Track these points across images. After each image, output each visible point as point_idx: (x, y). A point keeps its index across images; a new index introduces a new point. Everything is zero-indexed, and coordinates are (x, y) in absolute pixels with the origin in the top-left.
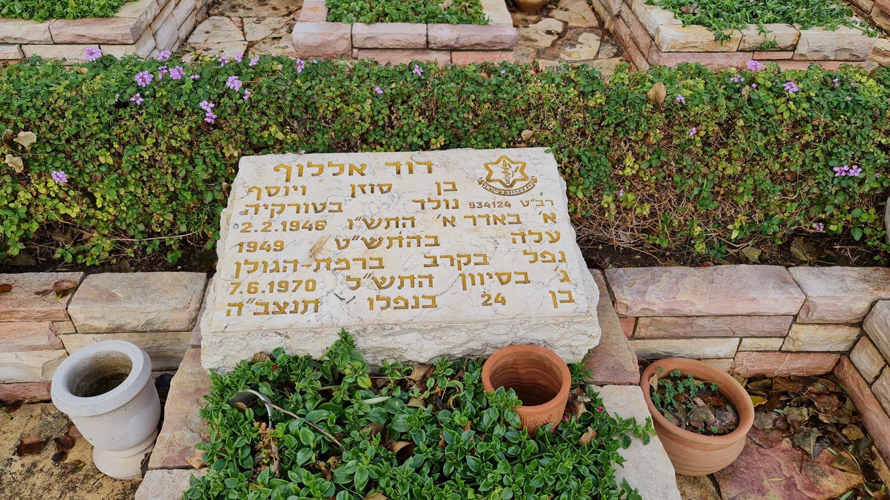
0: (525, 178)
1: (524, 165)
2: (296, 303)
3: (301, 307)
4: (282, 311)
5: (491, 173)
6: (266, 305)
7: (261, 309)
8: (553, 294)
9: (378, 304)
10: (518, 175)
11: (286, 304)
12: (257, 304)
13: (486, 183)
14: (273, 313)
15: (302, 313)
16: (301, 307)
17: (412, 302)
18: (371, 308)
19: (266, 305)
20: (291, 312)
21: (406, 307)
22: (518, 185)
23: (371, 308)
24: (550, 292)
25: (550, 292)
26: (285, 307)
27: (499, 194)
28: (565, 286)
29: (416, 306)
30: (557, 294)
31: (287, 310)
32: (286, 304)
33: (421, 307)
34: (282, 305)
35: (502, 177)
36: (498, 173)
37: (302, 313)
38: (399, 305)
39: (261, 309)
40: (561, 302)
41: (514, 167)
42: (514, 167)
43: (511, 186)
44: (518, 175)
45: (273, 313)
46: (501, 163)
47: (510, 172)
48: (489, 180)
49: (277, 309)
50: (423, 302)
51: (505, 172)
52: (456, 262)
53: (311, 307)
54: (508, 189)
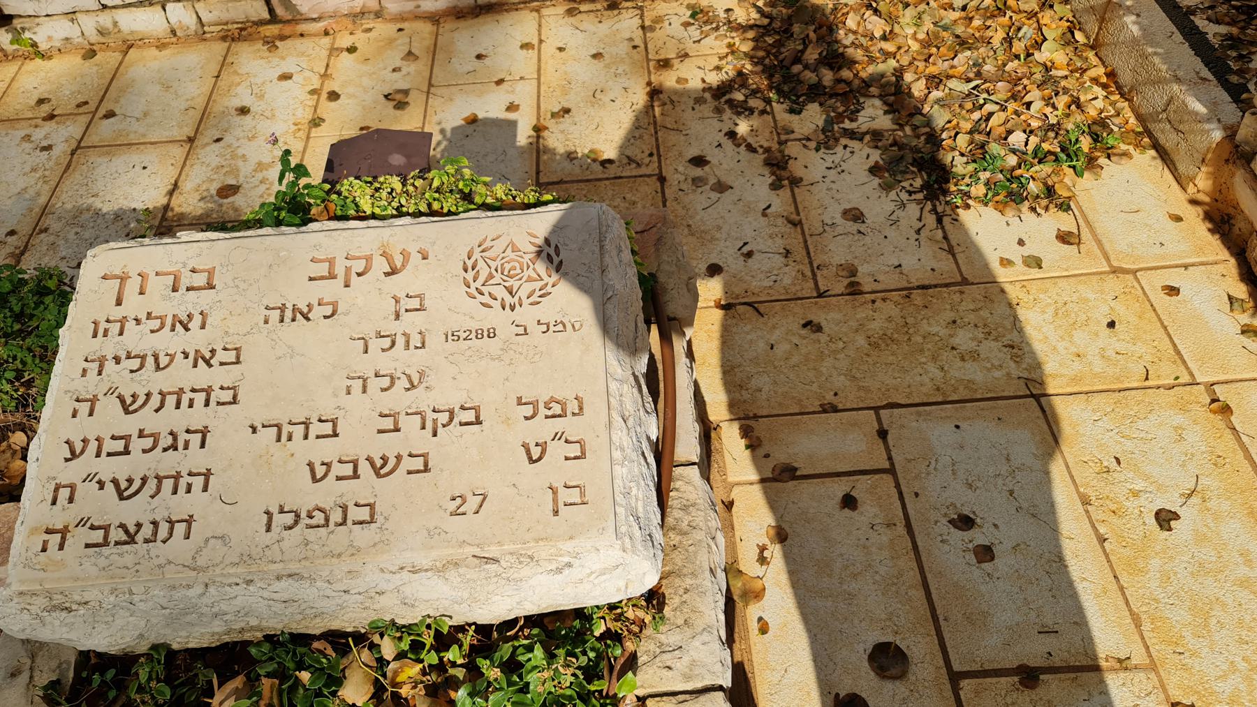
2: (155, 524)
4: (131, 540)
6: (106, 528)
7: (98, 536)
12: (93, 528)
17: (336, 516)
19: (106, 528)
20: (147, 541)
28: (574, 472)
30: (561, 491)
34: (132, 529)
38: (313, 522)
39: (98, 536)
49: (125, 538)
52: (429, 425)
53: (180, 529)
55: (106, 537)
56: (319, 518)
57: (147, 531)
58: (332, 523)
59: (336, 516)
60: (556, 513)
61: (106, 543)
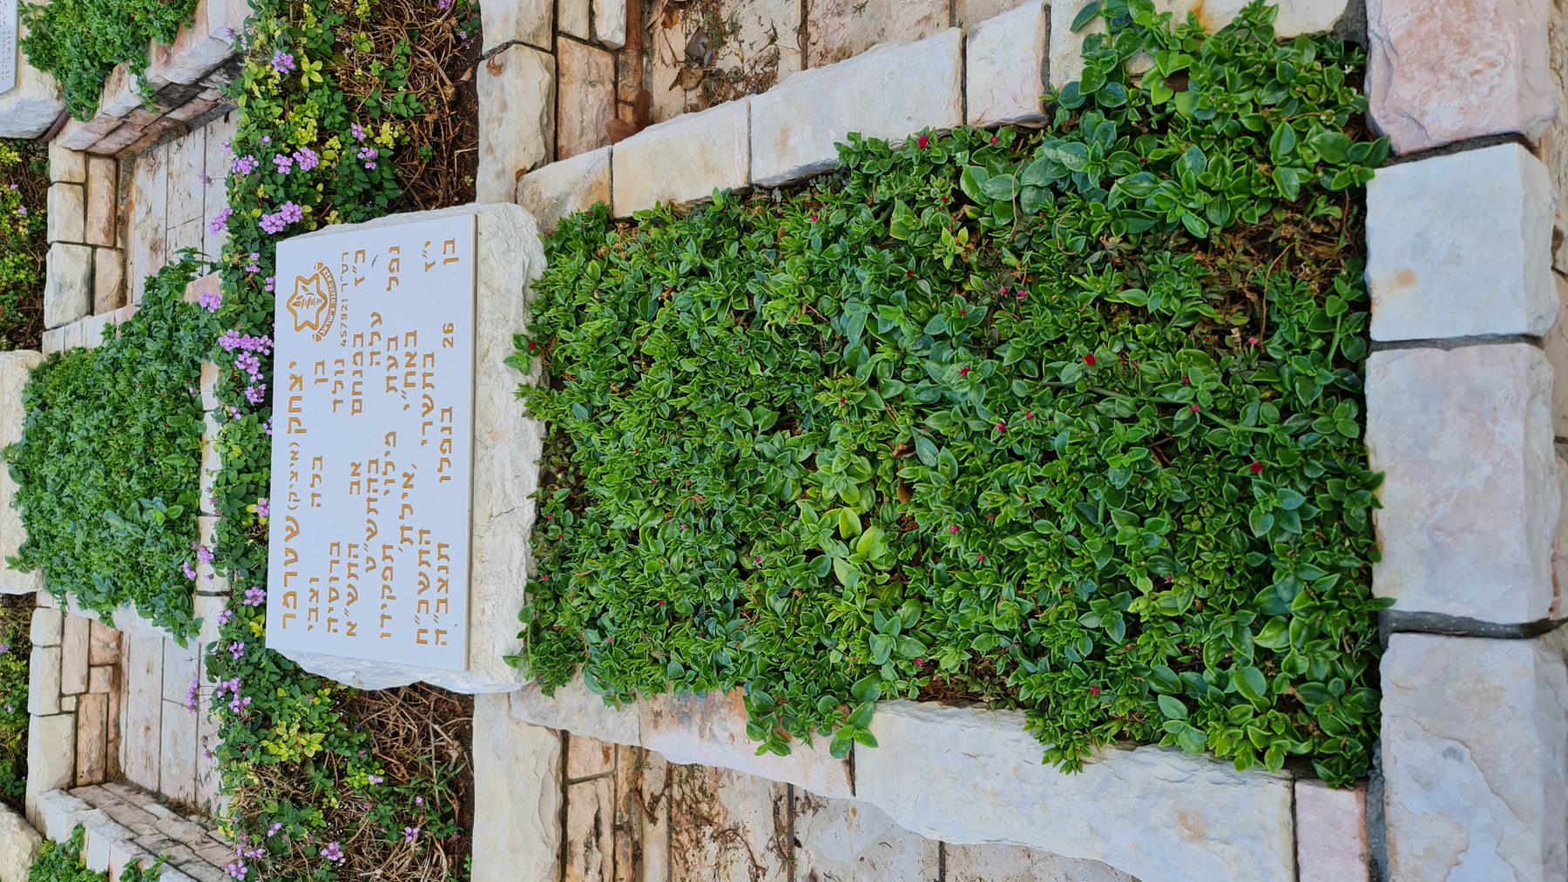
0: (316, 277)
1: (299, 278)
2: (440, 568)
3: (443, 562)
5: (307, 323)
8: (447, 260)
10: (312, 287)
17: (446, 434)
21: (449, 441)
22: (324, 289)
29: (449, 429)
35: (314, 308)
41: (301, 292)
42: (301, 292)
43: (324, 296)
48: (314, 327)
50: (446, 423)
51: (310, 302)
53: (444, 551)
54: (329, 302)
56: (446, 446)
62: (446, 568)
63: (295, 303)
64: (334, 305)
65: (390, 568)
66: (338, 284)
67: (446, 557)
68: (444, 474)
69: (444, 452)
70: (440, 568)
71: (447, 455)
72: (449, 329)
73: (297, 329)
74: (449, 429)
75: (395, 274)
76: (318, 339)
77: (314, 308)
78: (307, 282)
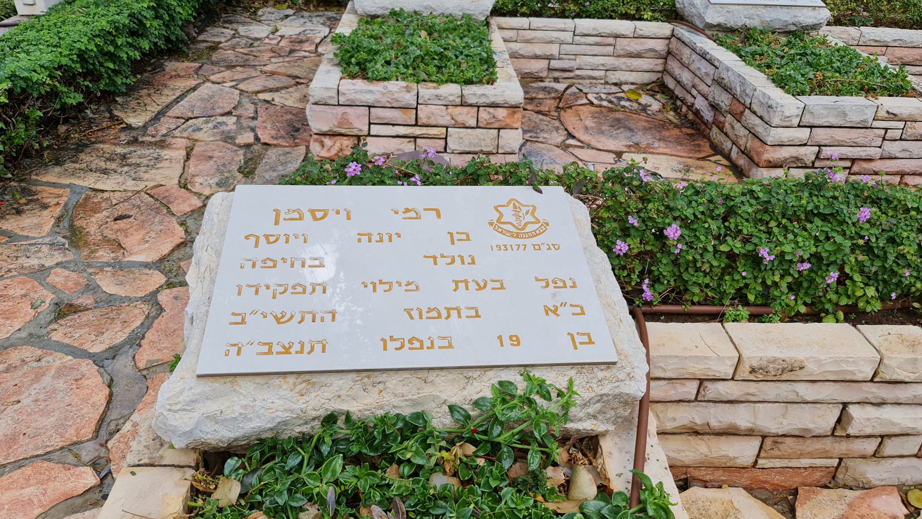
0: (538, 221)
1: (534, 208)
2: (302, 345)
3: (307, 348)
4: (287, 351)
5: (501, 215)
6: (270, 345)
7: (265, 349)
9: (391, 345)
11: (291, 345)
13: (497, 225)
14: (278, 353)
15: (309, 353)
16: (307, 348)
17: (427, 343)
18: (385, 349)
19: (270, 345)
20: (297, 352)
21: (422, 347)
23: (385, 349)
24: (569, 334)
25: (569, 334)
26: (290, 347)
27: (512, 236)
29: (432, 347)
31: (292, 350)
32: (291, 345)
33: (436, 347)
34: (287, 346)
35: (512, 219)
36: (508, 215)
37: (309, 353)
40: (581, 343)
42: (524, 210)
43: (523, 228)
44: (529, 218)
45: (278, 353)
46: (511, 205)
47: (521, 214)
51: (518, 217)
55: (270, 348)
57: (297, 347)
58: (425, 348)
59: (427, 343)
60: (576, 348)
61: (270, 352)
62: (301, 352)
63: (516, 206)
64: (517, 237)
65: (304, 292)
66: (536, 240)
67: (312, 350)
68: (389, 343)
69: (410, 342)
70: (302, 345)
71: (407, 345)
72: (516, 341)
73: (496, 208)
74: (432, 347)
75: (552, 285)
76: (491, 224)
77: (512, 219)
78: (533, 214)
